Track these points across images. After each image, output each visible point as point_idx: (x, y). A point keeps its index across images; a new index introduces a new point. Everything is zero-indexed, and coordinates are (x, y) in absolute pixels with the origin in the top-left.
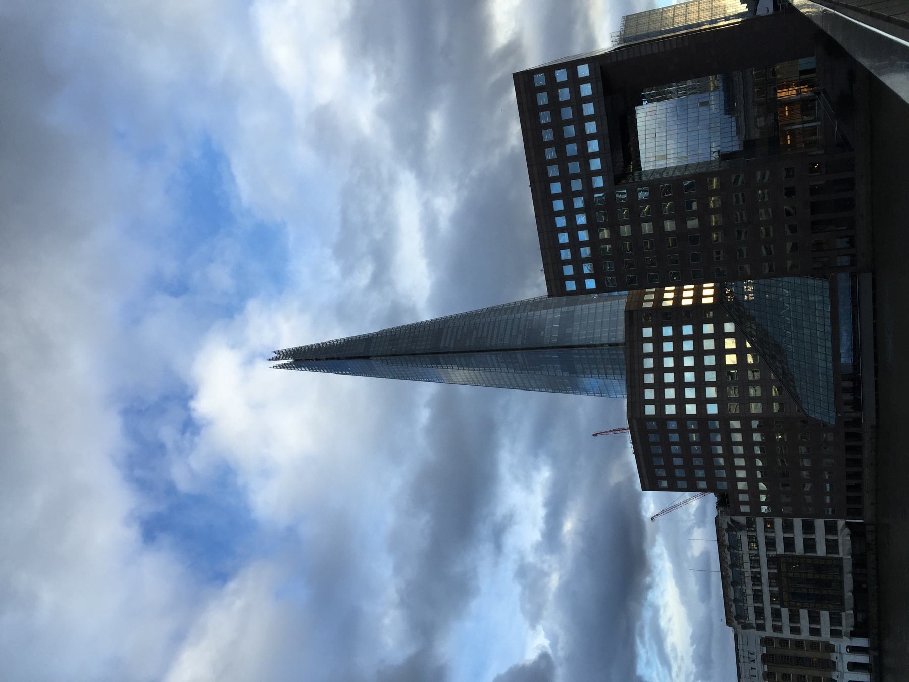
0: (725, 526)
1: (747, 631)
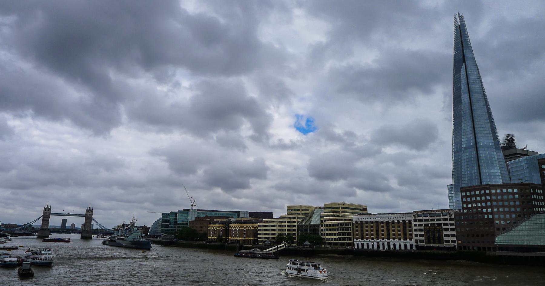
0: (450, 212)
1: (413, 217)
